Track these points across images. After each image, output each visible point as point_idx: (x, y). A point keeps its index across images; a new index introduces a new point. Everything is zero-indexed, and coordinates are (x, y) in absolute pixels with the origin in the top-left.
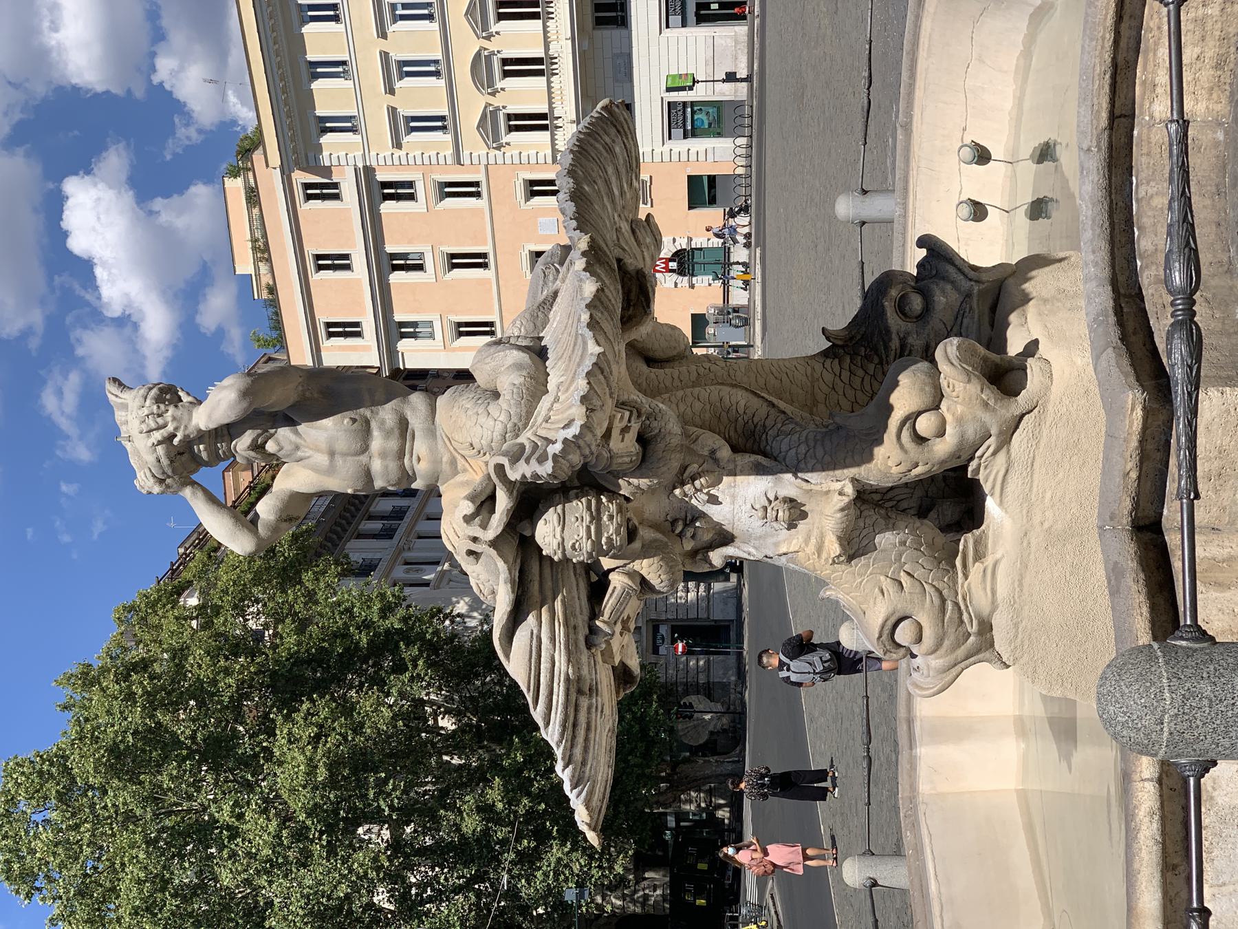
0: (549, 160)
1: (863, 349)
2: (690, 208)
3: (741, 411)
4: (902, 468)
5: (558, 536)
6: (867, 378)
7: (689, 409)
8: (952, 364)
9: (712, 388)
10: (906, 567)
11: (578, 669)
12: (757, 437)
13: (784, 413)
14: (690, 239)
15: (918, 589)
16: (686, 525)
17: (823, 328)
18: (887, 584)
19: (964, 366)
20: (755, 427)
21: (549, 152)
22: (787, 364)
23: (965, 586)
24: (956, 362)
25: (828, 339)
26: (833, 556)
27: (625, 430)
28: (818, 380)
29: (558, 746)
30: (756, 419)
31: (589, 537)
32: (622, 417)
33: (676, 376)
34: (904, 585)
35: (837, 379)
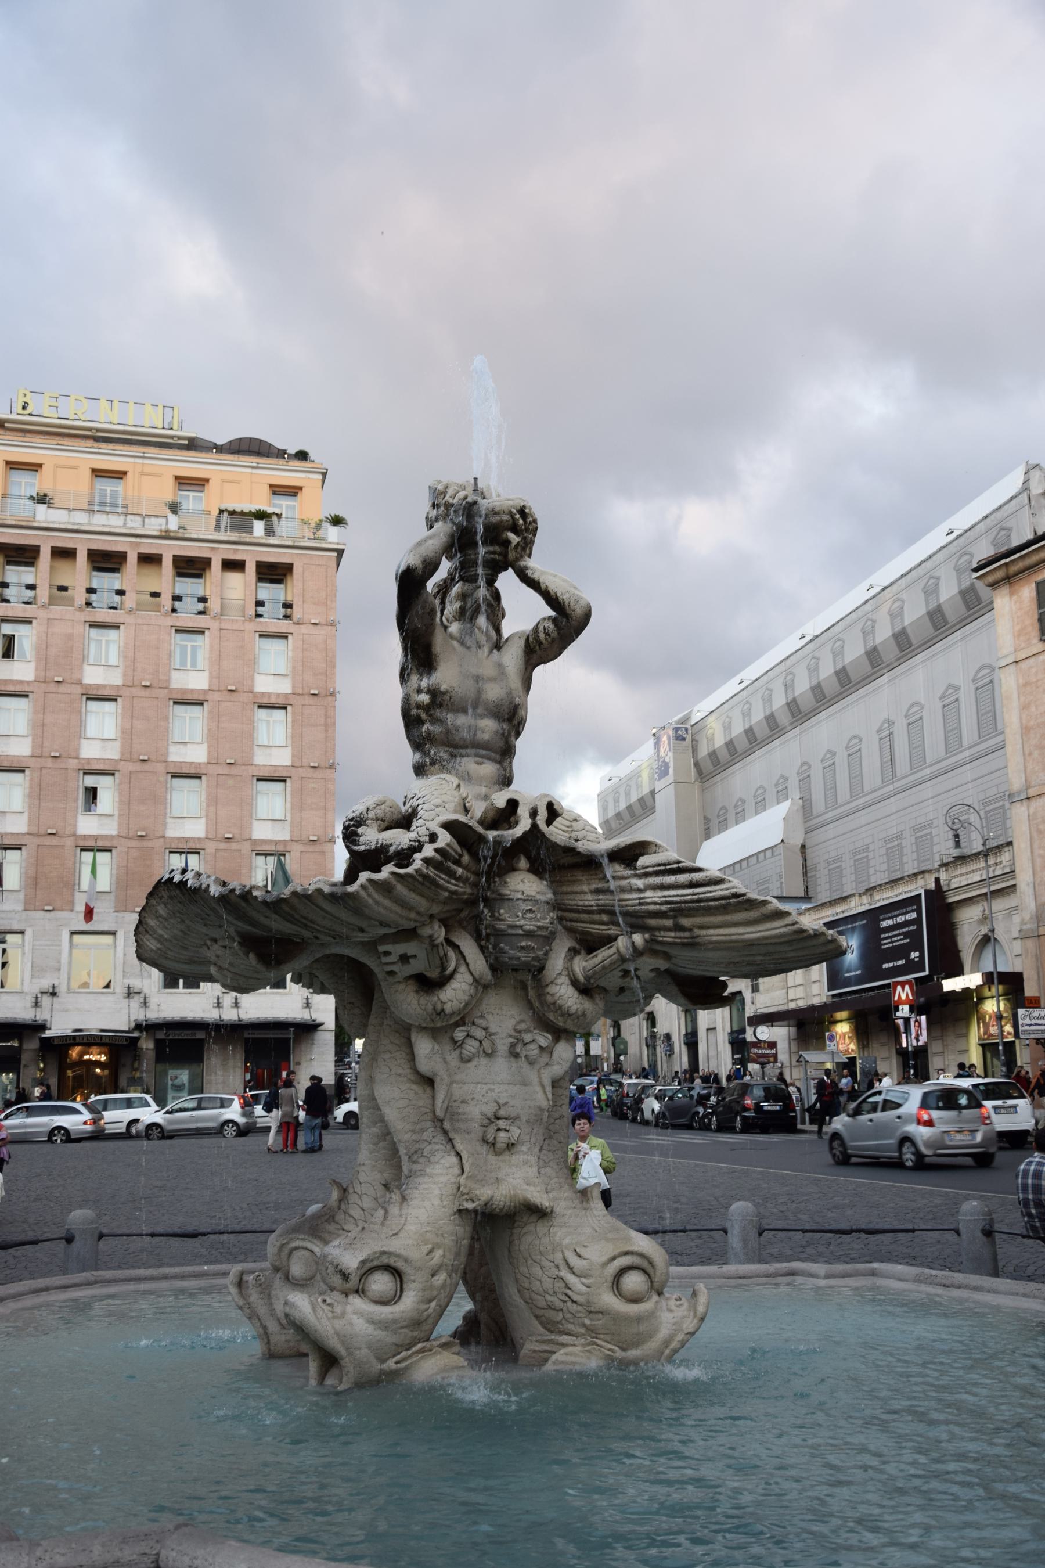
5: (538, 897)
15: (435, 1293)
16: (486, 1029)
18: (438, 1253)
29: (417, 871)
31: (539, 928)
34: (436, 1278)
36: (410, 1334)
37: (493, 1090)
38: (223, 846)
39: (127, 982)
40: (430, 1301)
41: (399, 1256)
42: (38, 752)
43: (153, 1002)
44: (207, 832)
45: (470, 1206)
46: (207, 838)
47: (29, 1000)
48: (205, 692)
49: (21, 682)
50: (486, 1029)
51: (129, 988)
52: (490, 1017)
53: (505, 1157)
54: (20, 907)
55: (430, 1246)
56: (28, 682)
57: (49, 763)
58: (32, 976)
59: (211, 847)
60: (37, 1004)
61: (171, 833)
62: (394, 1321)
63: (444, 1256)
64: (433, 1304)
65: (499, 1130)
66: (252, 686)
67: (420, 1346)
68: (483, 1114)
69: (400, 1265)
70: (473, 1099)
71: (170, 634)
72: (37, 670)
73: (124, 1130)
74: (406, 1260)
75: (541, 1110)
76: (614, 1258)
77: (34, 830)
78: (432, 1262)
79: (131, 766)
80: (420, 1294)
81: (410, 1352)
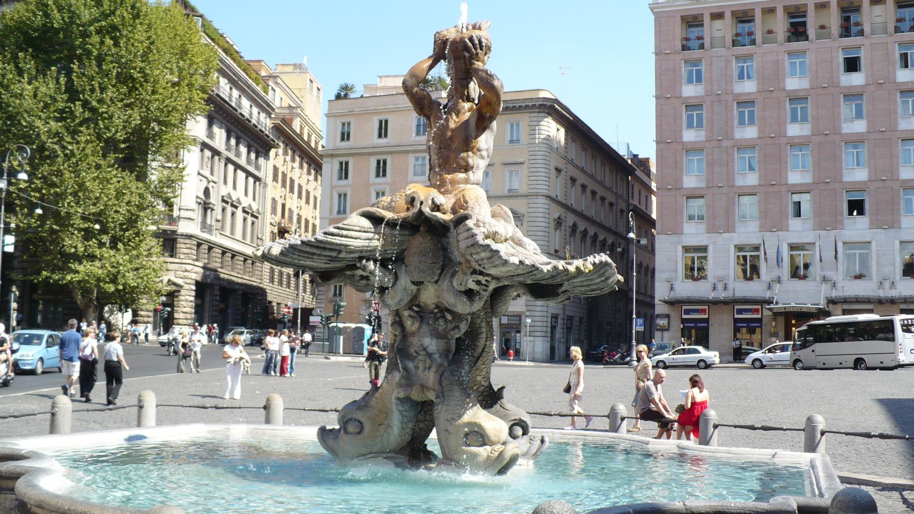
11: (352, 252)
17: (503, 388)
25: (499, 390)
27: (478, 283)
32: (486, 281)
38: (880, 184)
39: (823, 273)
42: (762, 135)
43: (839, 285)
44: (870, 176)
46: (870, 181)
47: (765, 286)
48: (863, 86)
49: (750, 94)
51: (824, 277)
54: (757, 229)
56: (753, 93)
57: (770, 141)
58: (767, 271)
59: (872, 187)
60: (769, 287)
61: (846, 179)
66: (895, 79)
71: (838, 52)
72: (758, 85)
73: (696, 364)
77: (763, 183)
79: (820, 138)
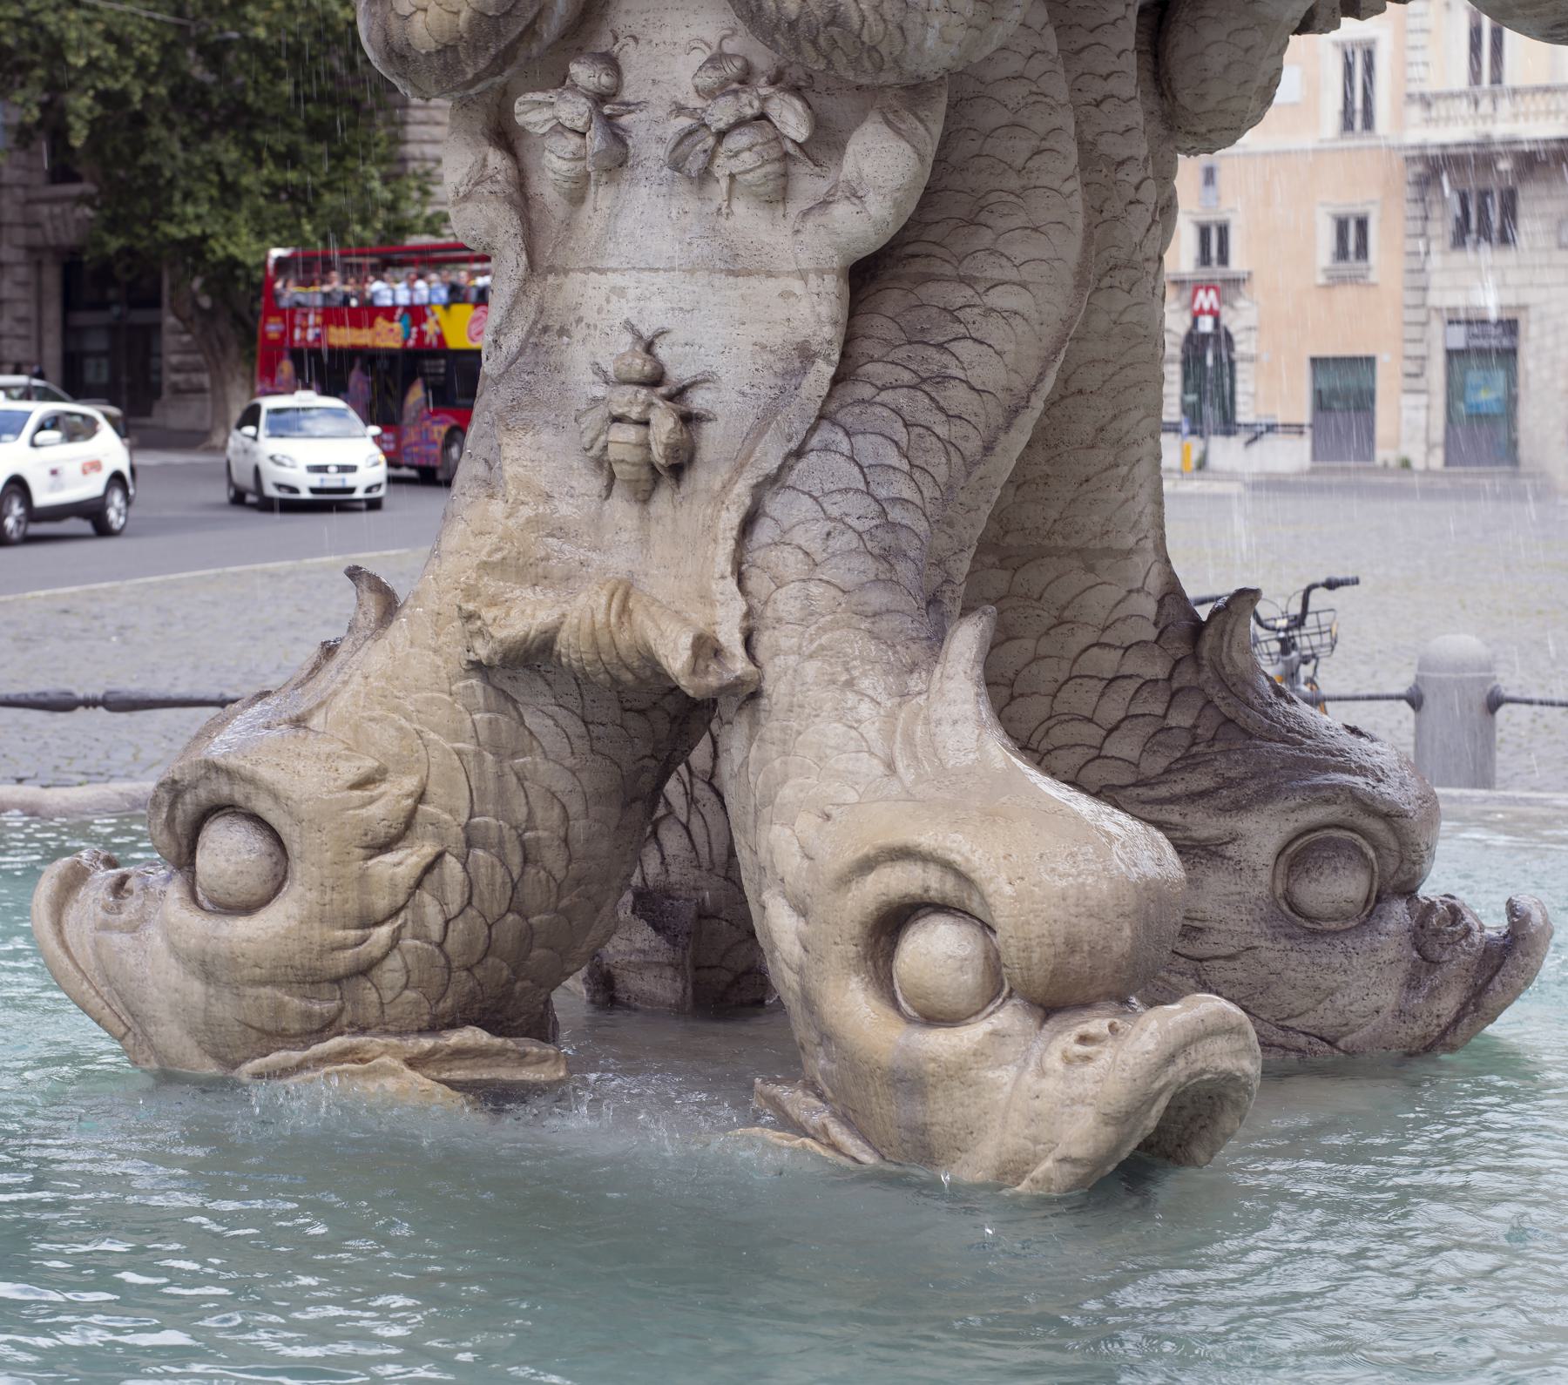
0: (1414, 88)
1: (1187, 721)
2: (1314, 361)
3: (1000, 299)
4: (790, 863)
6: (1092, 734)
7: (1006, 117)
8: (1171, 1059)
9: (1077, 202)
10: (452, 865)
12: (901, 354)
13: (988, 448)
14: (1251, 359)
15: (382, 903)
19: (1163, 1102)
20: (940, 346)
21: (1428, 88)
22: (1143, 470)
23: (386, 1060)
24: (1179, 1071)
26: (488, 614)
28: (1090, 569)
30: (965, 349)
33: (1112, 85)
34: (389, 858)
35: (1085, 637)
36: (295, 1003)
37: (620, 292)
40: (368, 922)
41: (251, 781)
45: (482, 651)
50: (600, 98)
52: (631, 57)
53: (662, 502)
55: (369, 764)
62: (233, 961)
63: (421, 797)
64: (383, 933)
65: (618, 419)
67: (335, 1043)
68: (598, 370)
69: (263, 806)
70: (580, 320)
74: (275, 797)
75: (806, 354)
76: (867, 865)
78: (376, 810)
80: (313, 896)
81: (296, 1056)
